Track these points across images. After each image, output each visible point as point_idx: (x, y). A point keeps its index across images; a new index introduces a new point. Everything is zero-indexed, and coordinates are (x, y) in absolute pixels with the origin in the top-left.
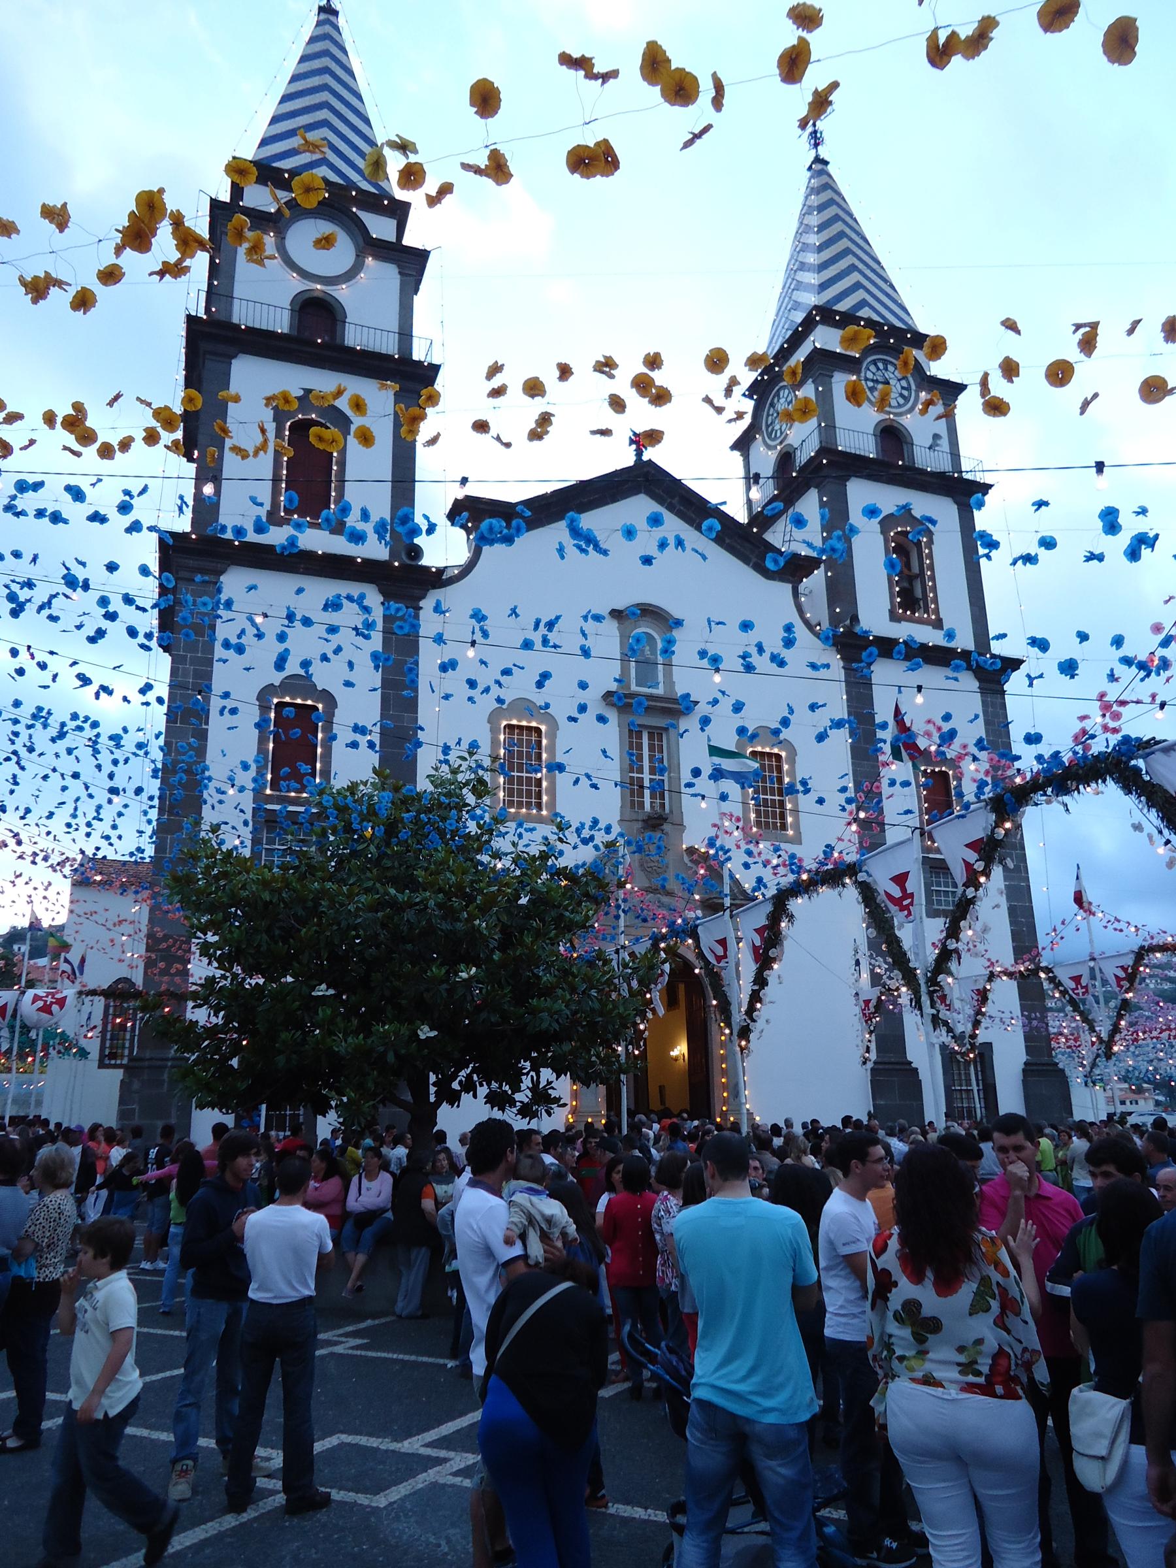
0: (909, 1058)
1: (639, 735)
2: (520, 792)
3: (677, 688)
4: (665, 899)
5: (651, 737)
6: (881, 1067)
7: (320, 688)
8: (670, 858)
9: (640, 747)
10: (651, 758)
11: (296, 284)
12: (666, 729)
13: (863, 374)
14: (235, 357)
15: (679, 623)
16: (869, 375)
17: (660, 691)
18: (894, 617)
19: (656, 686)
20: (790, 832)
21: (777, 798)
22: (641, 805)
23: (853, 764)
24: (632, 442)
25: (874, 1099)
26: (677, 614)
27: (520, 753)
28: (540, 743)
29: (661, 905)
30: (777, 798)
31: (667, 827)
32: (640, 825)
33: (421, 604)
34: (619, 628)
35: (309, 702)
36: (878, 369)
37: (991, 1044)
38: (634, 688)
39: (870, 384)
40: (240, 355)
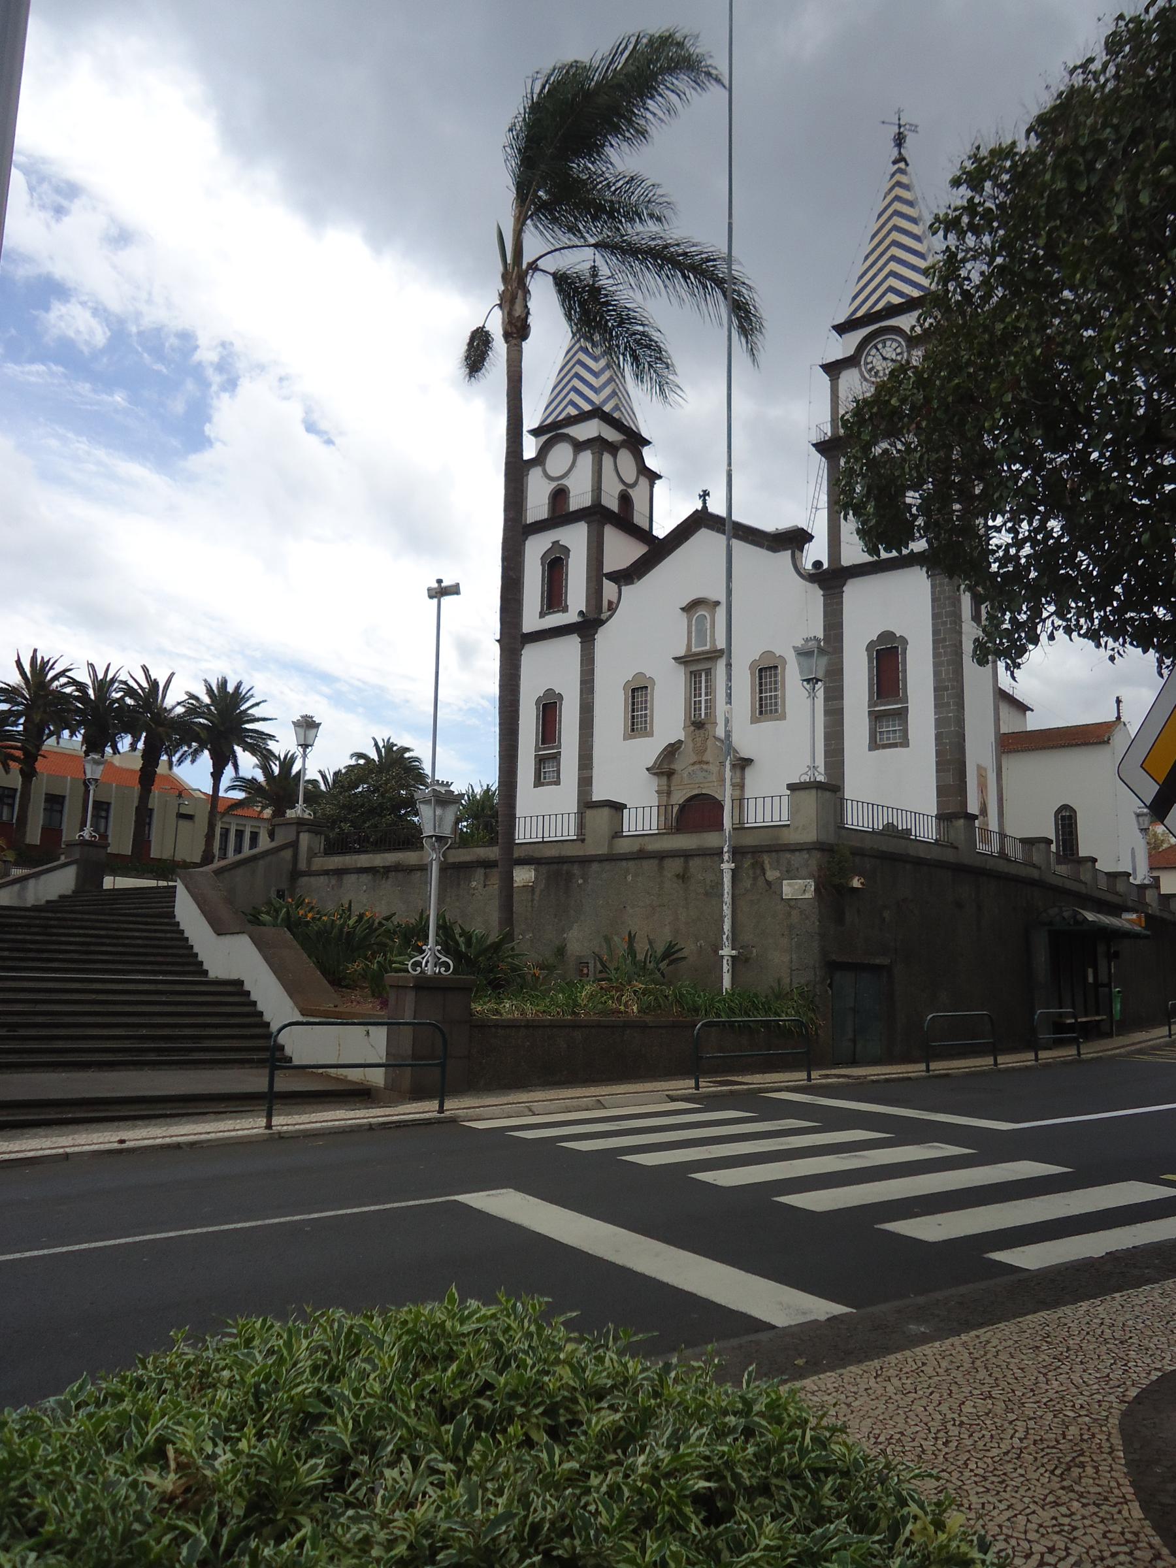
3: (717, 643)
4: (705, 767)
5: (706, 676)
8: (709, 743)
10: (706, 687)
11: (551, 486)
13: (862, 363)
14: (526, 539)
16: (869, 360)
17: (707, 648)
24: (700, 496)
29: (702, 770)
31: (706, 726)
36: (878, 350)
38: (694, 650)
39: (869, 366)
40: (530, 538)
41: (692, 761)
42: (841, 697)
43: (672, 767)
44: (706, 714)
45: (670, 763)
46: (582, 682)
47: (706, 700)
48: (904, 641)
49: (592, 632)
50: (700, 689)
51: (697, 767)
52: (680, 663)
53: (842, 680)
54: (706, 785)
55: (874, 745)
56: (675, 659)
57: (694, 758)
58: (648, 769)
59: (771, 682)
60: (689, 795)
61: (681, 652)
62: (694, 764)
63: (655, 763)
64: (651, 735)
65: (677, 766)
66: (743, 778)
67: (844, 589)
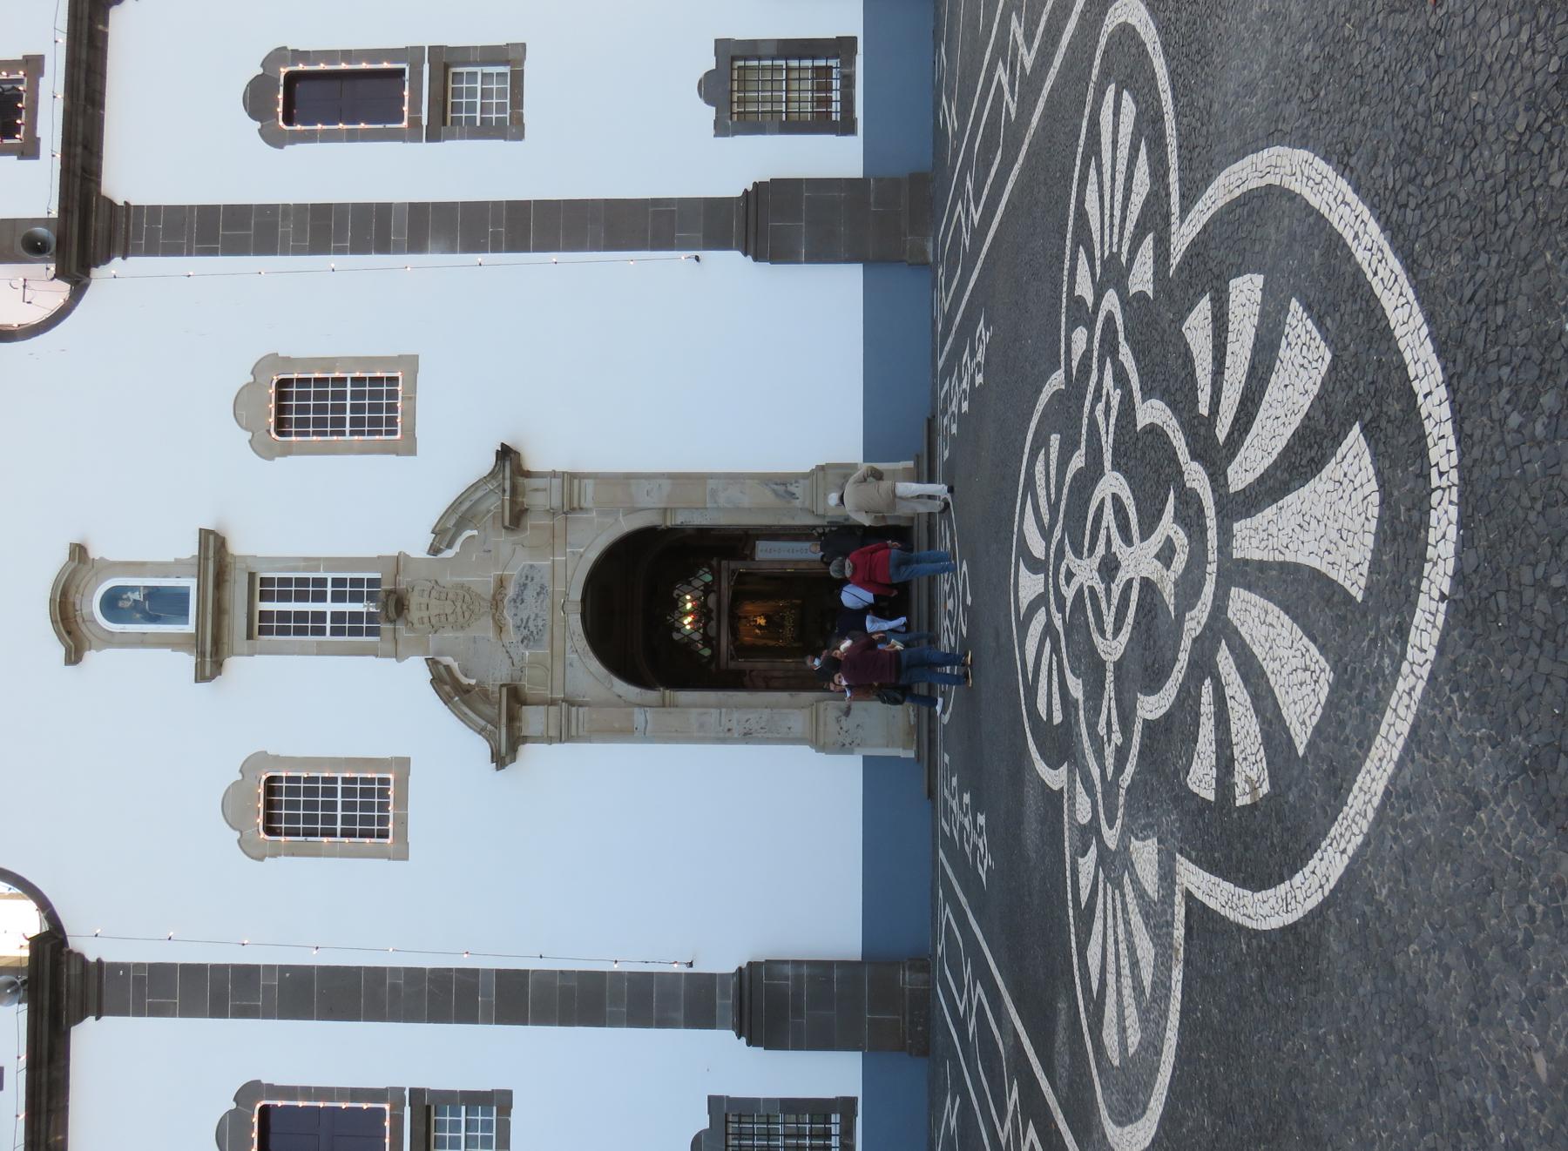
0: (739, 193)
1: (264, 615)
2: (370, 807)
4: (511, 591)
5: (265, 597)
6: (752, 247)
7: (234, 1106)
8: (448, 579)
9: (284, 616)
10: (301, 597)
12: (252, 576)
15: (79, 552)
17: (191, 583)
18: (30, 150)
19: (188, 588)
20: (399, 374)
21: (349, 389)
22: (371, 617)
23: (285, 252)
25: (798, 262)
26: (59, 557)
27: (308, 806)
28: (289, 779)
29: (519, 599)
30: (349, 389)
31: (403, 586)
32: (400, 626)
33: (92, 958)
34: (98, 650)
35: (255, 1120)
37: (716, 41)
38: (190, 628)
41: (491, 634)
42: (384, 210)
43: (497, 689)
44: (371, 597)
45: (485, 695)
46: (218, 1010)
47: (338, 597)
48: (279, 56)
49: (75, 970)
50: (301, 616)
51: (510, 622)
52: (218, 667)
53: (341, 208)
54: (560, 588)
55: (511, 128)
56: (201, 677)
57: (484, 628)
58: (501, 759)
59: (323, 409)
60: (582, 643)
61: (185, 662)
62: (500, 629)
63: (481, 731)
64: (403, 765)
65: (497, 673)
66: (554, 474)
67: (120, 202)
